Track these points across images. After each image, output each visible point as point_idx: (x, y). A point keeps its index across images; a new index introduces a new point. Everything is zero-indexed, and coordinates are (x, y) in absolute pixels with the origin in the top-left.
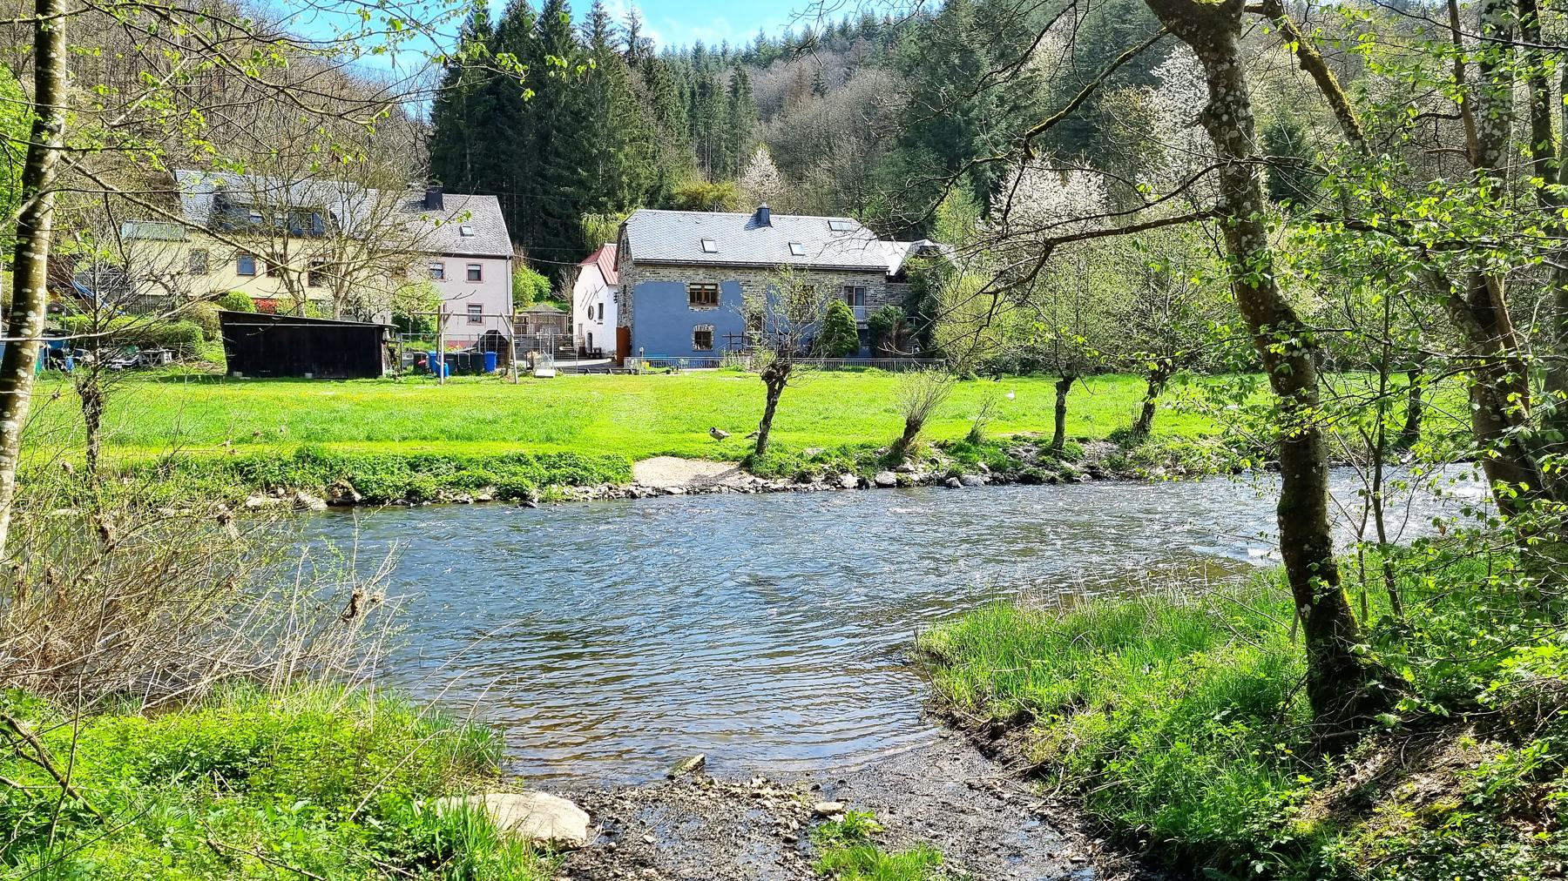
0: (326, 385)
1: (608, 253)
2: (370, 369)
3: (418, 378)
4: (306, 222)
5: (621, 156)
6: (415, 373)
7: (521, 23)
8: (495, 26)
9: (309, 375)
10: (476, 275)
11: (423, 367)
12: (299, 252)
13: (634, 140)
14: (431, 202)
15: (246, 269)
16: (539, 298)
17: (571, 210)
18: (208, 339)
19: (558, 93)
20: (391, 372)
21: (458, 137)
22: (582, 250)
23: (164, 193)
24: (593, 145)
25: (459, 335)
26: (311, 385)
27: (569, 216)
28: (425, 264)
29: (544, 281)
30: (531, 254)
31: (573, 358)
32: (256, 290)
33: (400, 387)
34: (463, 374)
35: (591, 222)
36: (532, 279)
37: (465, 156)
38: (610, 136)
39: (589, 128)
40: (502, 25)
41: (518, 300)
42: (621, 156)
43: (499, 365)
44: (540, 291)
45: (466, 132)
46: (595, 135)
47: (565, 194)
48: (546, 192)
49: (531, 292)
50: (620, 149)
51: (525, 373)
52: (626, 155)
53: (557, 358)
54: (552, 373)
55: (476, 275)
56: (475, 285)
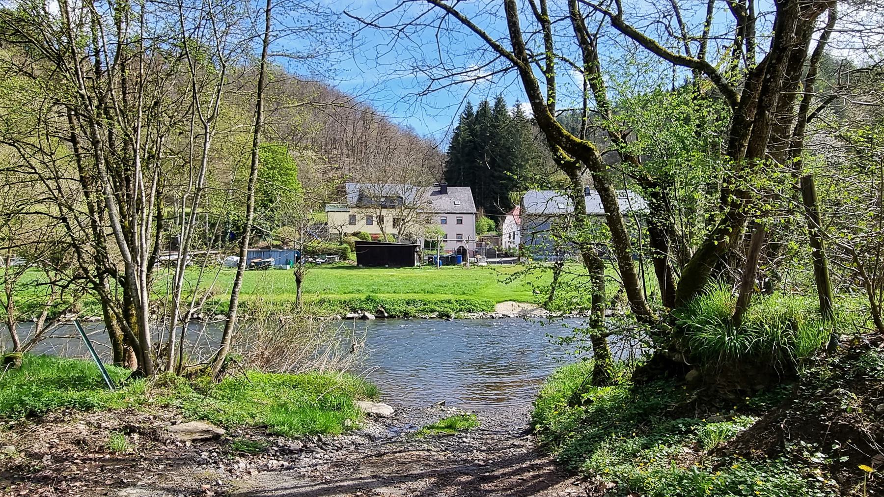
0: (393, 270)
1: (516, 212)
2: (411, 264)
3: (429, 267)
4: (390, 202)
5: (527, 166)
6: (428, 265)
7: (485, 112)
8: (475, 113)
9: (387, 266)
10: (460, 222)
11: (431, 262)
12: (389, 215)
13: (534, 158)
14: (443, 191)
15: (369, 222)
16: (490, 230)
17: (505, 191)
18: (352, 251)
19: (500, 140)
20: (419, 264)
21: (458, 162)
22: (509, 208)
23: (340, 193)
24: (514, 162)
25: (449, 248)
26: (387, 270)
27: (504, 193)
28: (438, 219)
29: (492, 222)
30: (486, 211)
31: (495, 257)
32: (371, 230)
33: (421, 271)
34: (448, 265)
35: (513, 195)
36: (486, 221)
37: (460, 169)
38: (523, 157)
39: (513, 154)
40: (477, 112)
41: (479, 231)
42: (527, 166)
43: (463, 261)
44: (490, 227)
45: (461, 159)
46: (516, 157)
47: (502, 183)
48: (494, 183)
49: (486, 228)
50: (527, 162)
51: (474, 264)
52: (530, 165)
53: (487, 257)
54: (485, 264)
55: (460, 222)
56: (460, 226)
